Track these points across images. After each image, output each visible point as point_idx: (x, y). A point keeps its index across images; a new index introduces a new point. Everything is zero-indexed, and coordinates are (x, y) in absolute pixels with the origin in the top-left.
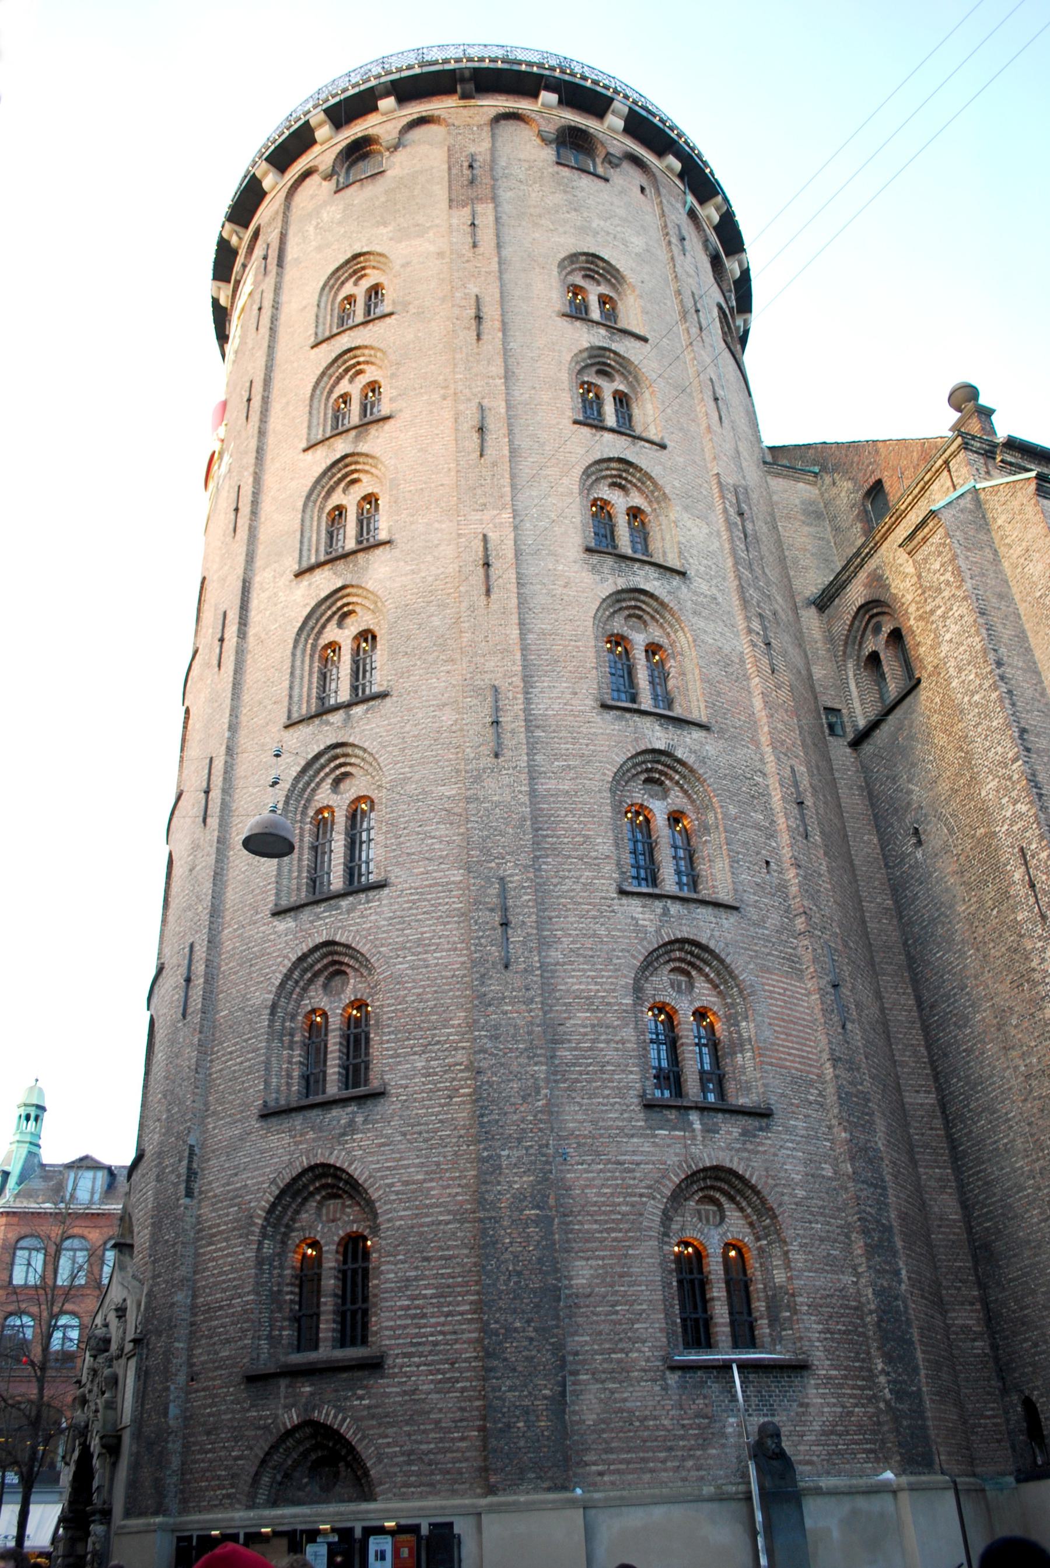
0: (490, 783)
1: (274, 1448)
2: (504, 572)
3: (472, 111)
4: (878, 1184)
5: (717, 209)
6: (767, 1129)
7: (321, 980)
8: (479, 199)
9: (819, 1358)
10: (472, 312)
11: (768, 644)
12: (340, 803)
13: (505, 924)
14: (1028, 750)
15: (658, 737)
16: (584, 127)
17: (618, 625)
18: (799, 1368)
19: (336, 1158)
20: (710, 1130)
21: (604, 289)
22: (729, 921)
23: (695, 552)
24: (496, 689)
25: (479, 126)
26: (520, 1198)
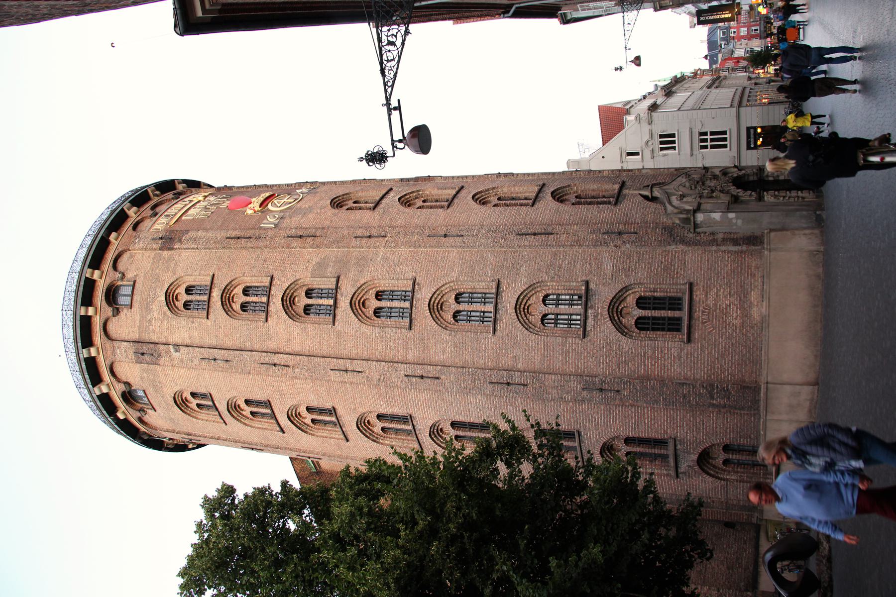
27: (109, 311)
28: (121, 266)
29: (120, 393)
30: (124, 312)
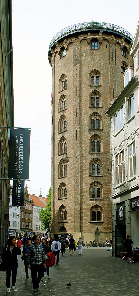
9: (105, 222)
16: (95, 38)
17: (93, 140)
21: (97, 75)
22: (102, 178)
26: (77, 208)
27: (89, 41)
29: (64, 46)
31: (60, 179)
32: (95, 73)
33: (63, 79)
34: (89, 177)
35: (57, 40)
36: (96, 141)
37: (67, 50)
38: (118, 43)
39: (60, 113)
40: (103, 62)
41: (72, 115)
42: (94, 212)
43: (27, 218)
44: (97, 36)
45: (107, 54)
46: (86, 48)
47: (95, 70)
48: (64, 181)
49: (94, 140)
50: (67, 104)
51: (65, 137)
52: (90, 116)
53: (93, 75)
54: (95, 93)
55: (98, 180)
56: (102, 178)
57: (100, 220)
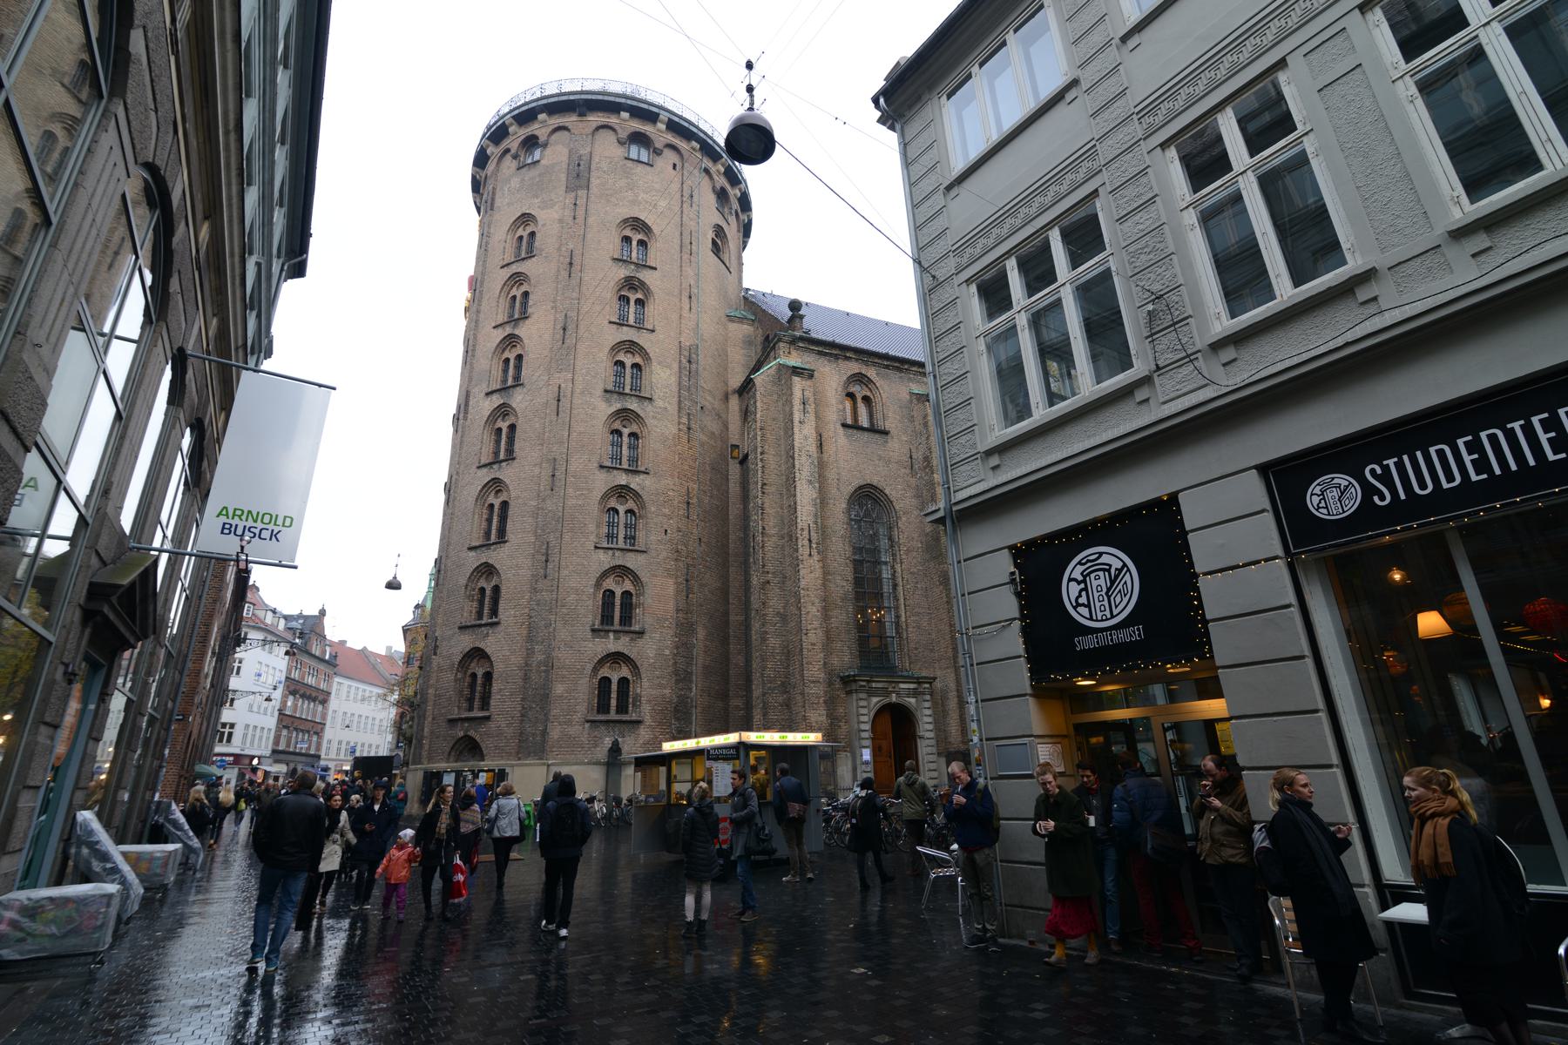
0: (548, 502)
1: (456, 743)
2: (565, 403)
3: (585, 124)
4: (689, 659)
5: (723, 165)
6: (641, 638)
7: (484, 576)
8: (581, 187)
9: (648, 719)
10: (568, 260)
11: (689, 429)
12: (497, 503)
13: (547, 561)
14: (763, 493)
15: (622, 479)
17: (617, 425)
18: (639, 722)
19: (482, 645)
20: (616, 639)
21: (640, 237)
22: (641, 558)
23: (659, 386)
24: (555, 459)
25: (587, 135)
26: (540, 663)
27: (623, 135)
28: (668, 153)
29: (536, 133)
30: (620, 152)
31: (478, 551)
32: (634, 228)
33: (521, 229)
34: (596, 547)
35: (511, 111)
36: (626, 431)
37: (545, 145)
38: (707, 171)
39: (500, 330)
40: (663, 204)
41: (547, 337)
42: (606, 682)
43: (308, 715)
44: (647, 128)
45: (676, 186)
46: (607, 150)
47: (636, 219)
48: (496, 557)
49: (620, 428)
50: (531, 303)
51: (514, 405)
52: (613, 349)
53: (628, 232)
54: (631, 283)
55: (631, 561)
56: (644, 555)
57: (627, 712)
